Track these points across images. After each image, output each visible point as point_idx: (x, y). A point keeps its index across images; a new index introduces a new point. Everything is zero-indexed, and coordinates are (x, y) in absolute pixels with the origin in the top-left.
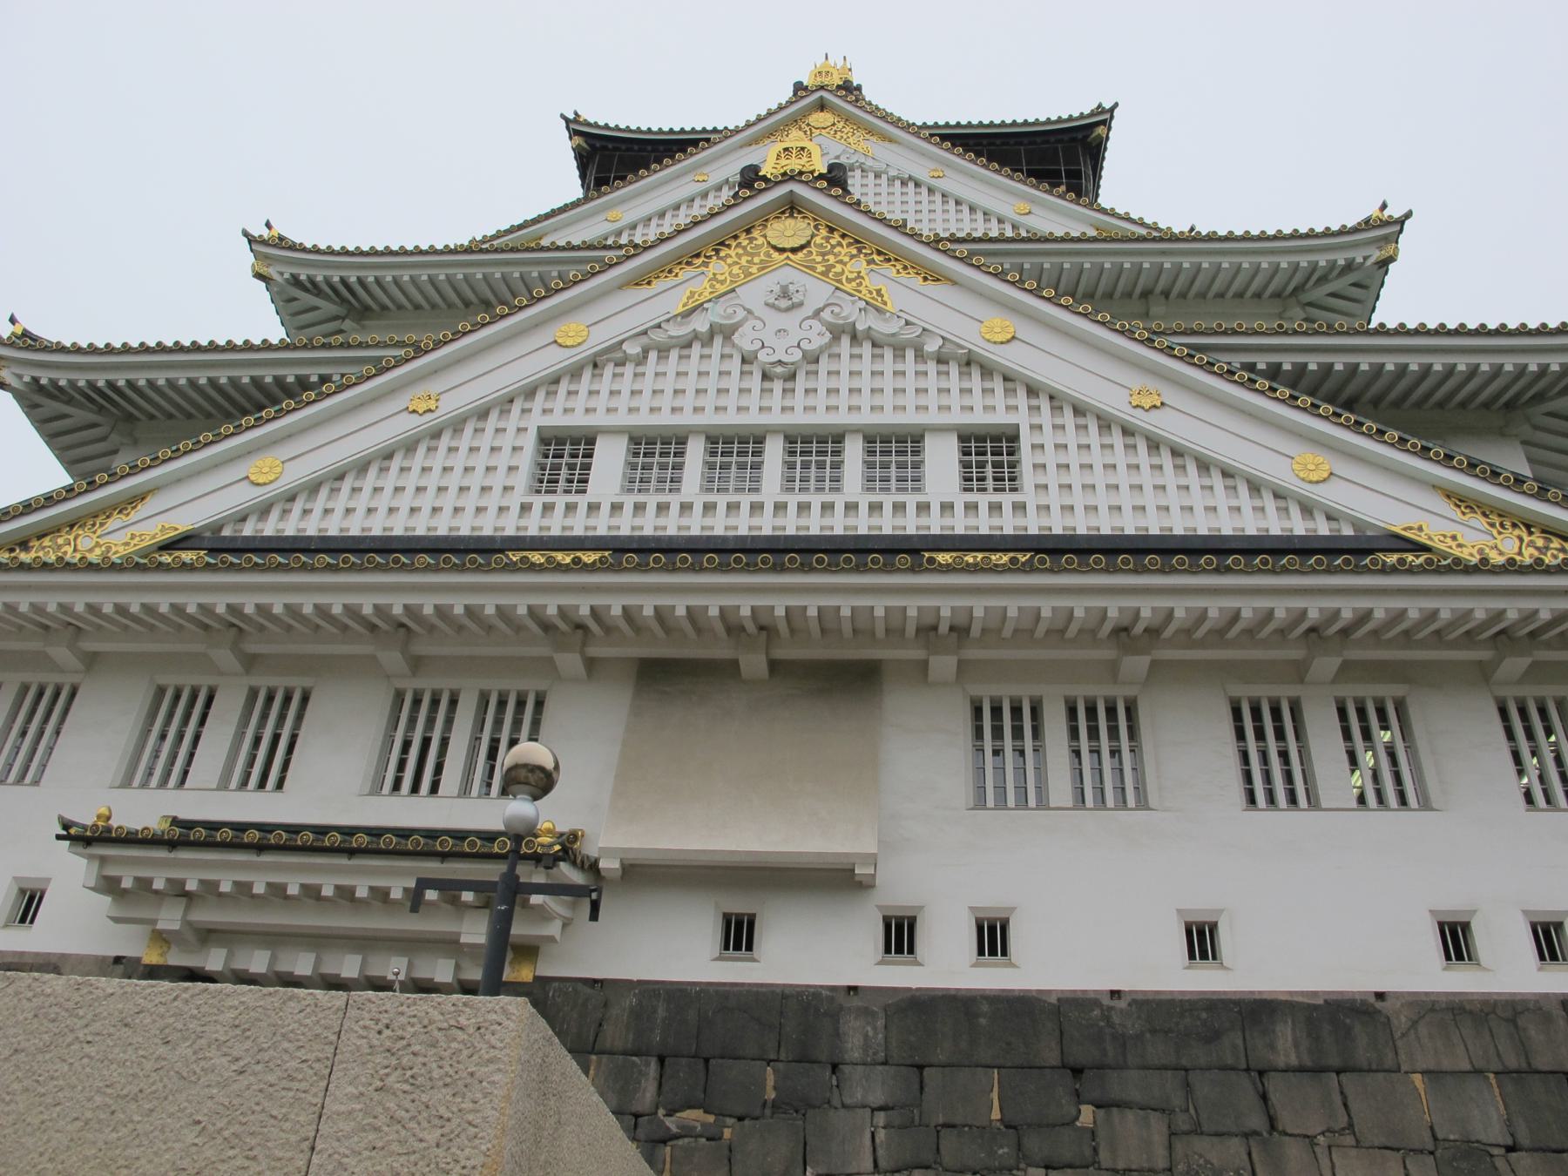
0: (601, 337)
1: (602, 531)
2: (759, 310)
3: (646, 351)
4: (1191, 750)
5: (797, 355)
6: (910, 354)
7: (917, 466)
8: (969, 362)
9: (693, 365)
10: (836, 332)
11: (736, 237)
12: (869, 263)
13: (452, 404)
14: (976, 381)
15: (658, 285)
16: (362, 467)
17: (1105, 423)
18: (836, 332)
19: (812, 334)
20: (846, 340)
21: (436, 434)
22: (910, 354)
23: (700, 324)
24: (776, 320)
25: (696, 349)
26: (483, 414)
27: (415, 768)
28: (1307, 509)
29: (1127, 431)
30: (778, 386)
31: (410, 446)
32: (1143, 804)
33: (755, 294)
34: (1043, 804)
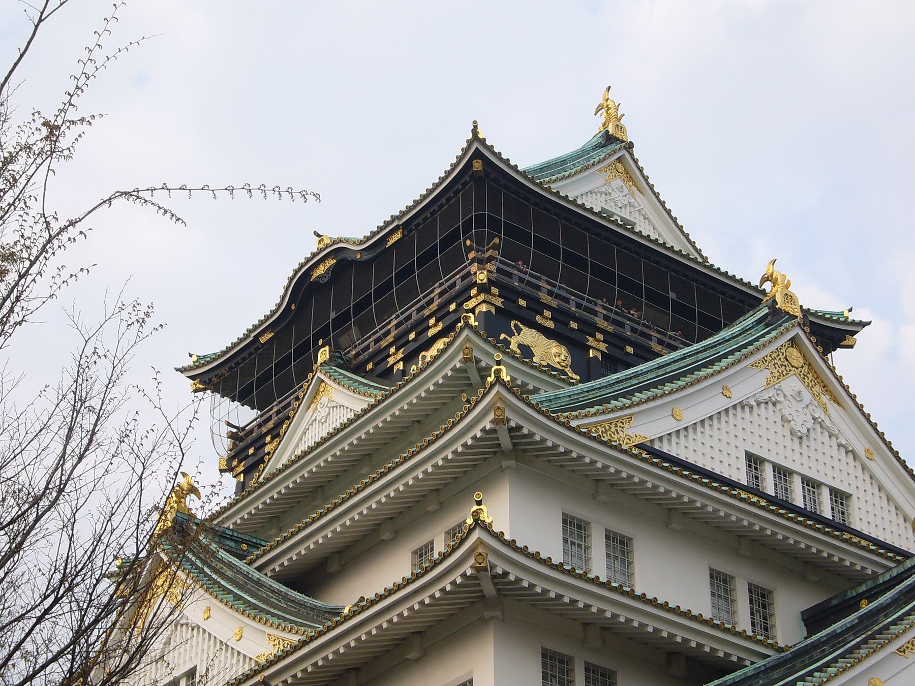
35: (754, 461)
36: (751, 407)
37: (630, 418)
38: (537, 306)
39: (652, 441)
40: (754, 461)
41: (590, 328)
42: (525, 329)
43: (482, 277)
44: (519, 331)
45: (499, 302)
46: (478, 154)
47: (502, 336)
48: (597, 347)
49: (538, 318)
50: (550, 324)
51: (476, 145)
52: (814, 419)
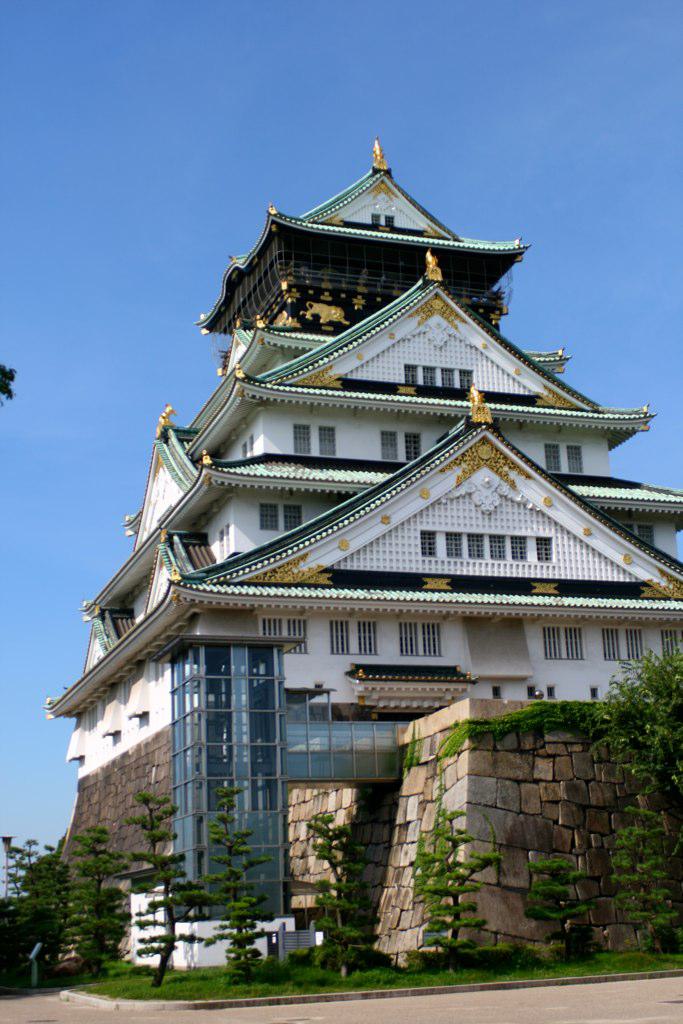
0: (435, 494)
1: (446, 572)
2: (480, 488)
4: (593, 644)
5: (492, 508)
10: (501, 496)
12: (510, 468)
14: (540, 519)
15: (448, 472)
17: (575, 538)
18: (501, 496)
22: (522, 507)
23: (462, 491)
25: (461, 500)
26: (403, 524)
27: (406, 647)
28: (624, 571)
29: (581, 541)
30: (486, 517)
31: (384, 536)
32: (582, 659)
34: (561, 659)
35: (410, 369)
36: (409, 340)
38: (319, 291)
39: (346, 374)
40: (410, 369)
41: (355, 294)
42: (315, 305)
43: (284, 286)
44: (311, 306)
45: (298, 295)
46: (273, 222)
47: (301, 313)
48: (359, 303)
49: (322, 298)
50: (330, 299)
51: (271, 218)
52: (450, 336)
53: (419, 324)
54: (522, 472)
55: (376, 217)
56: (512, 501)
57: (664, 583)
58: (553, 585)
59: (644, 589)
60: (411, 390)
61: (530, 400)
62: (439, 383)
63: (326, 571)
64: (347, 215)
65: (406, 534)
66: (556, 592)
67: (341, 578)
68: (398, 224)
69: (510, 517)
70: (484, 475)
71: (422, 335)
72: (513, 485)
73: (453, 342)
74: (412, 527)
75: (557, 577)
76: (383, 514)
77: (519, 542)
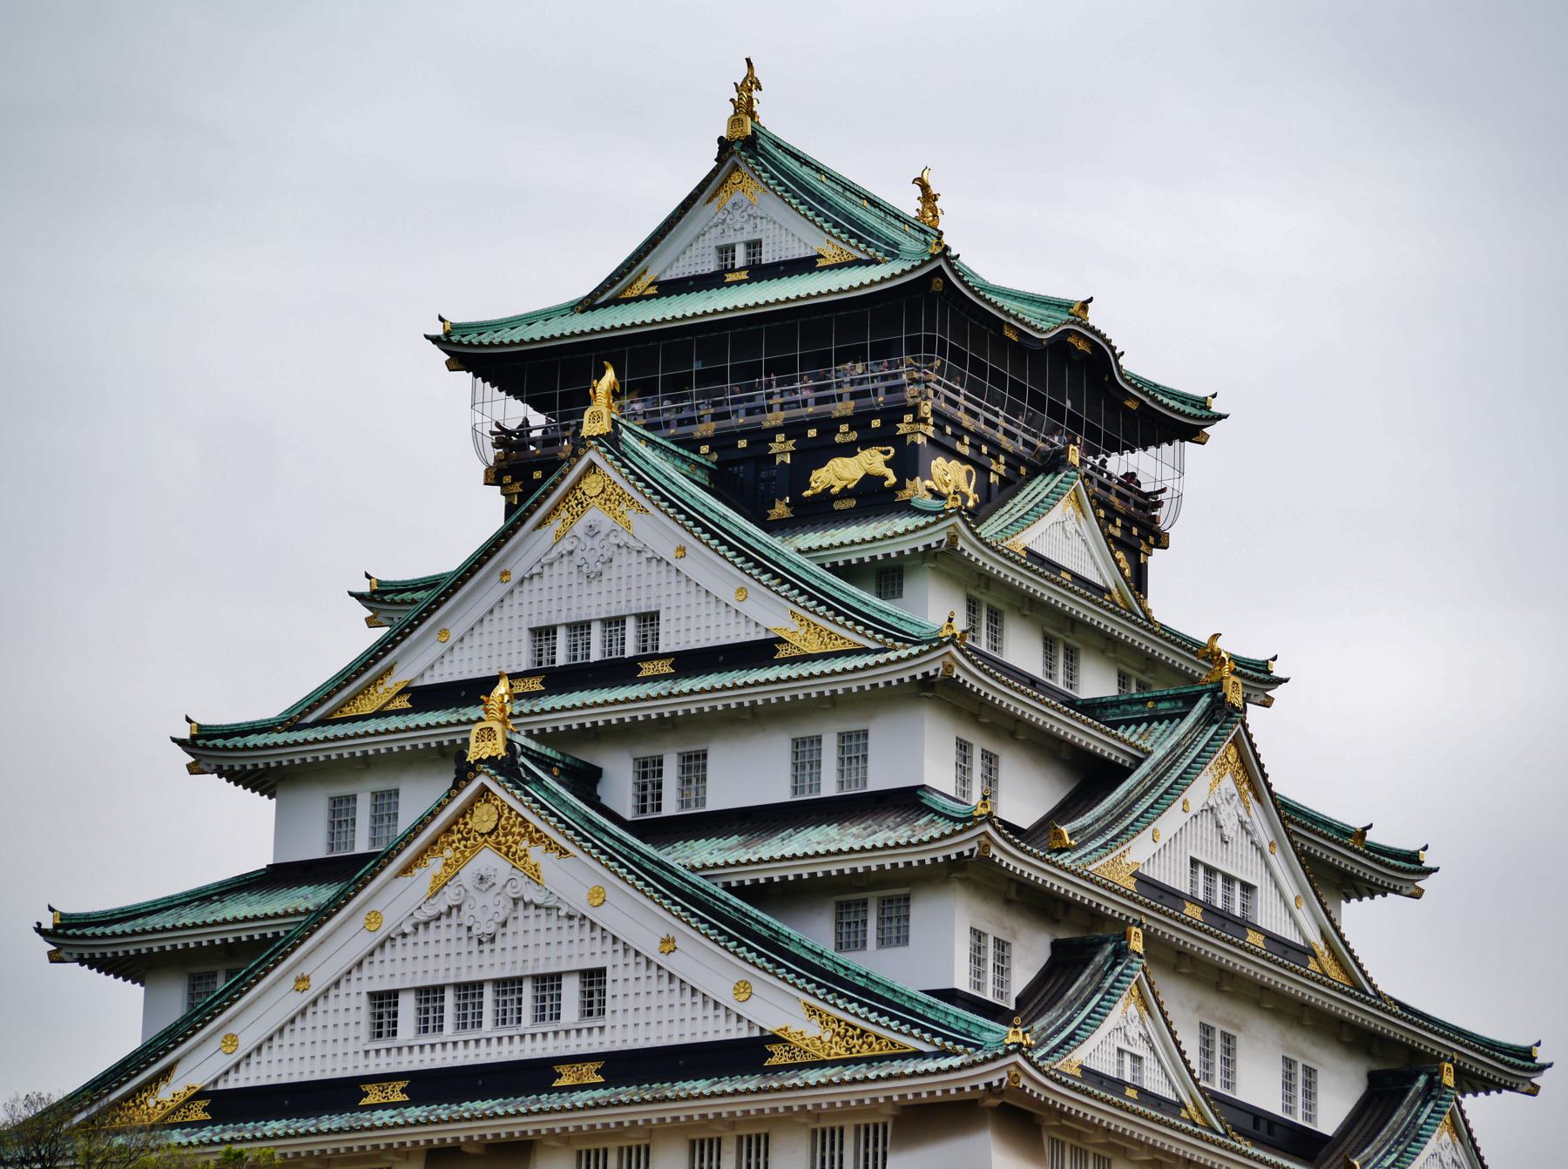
1: (405, 1067)
3: (416, 927)
6: (554, 913)
7: (559, 996)
8: (584, 917)
9: (443, 934)
10: (515, 901)
11: (456, 823)
12: (532, 840)
13: (317, 985)
15: (416, 871)
16: (281, 1030)
17: (649, 962)
18: (515, 901)
19: (499, 909)
20: (521, 905)
21: (315, 1002)
24: (482, 899)
26: (337, 984)
28: (739, 1018)
29: (659, 967)
31: (303, 1012)
33: (467, 874)
36: (540, 574)
37: (389, 670)
39: (422, 675)
40: (543, 634)
53: (559, 538)
54: (551, 846)
55: (726, 251)
56: (537, 907)
57: (812, 1029)
58: (593, 1066)
59: (773, 1048)
60: (535, 685)
61: (761, 652)
62: (596, 655)
63: (200, 1095)
64: (664, 266)
65: (342, 1003)
66: (600, 1079)
67: (227, 1105)
68: (767, 258)
69: (531, 939)
70: (487, 860)
71: (565, 559)
72: (534, 876)
73: (623, 558)
74: (354, 986)
75: (607, 1047)
76: (297, 973)
77: (549, 983)
